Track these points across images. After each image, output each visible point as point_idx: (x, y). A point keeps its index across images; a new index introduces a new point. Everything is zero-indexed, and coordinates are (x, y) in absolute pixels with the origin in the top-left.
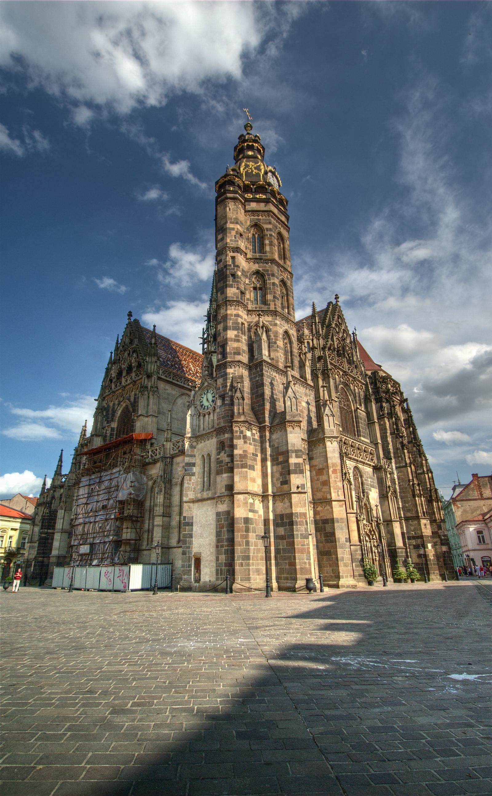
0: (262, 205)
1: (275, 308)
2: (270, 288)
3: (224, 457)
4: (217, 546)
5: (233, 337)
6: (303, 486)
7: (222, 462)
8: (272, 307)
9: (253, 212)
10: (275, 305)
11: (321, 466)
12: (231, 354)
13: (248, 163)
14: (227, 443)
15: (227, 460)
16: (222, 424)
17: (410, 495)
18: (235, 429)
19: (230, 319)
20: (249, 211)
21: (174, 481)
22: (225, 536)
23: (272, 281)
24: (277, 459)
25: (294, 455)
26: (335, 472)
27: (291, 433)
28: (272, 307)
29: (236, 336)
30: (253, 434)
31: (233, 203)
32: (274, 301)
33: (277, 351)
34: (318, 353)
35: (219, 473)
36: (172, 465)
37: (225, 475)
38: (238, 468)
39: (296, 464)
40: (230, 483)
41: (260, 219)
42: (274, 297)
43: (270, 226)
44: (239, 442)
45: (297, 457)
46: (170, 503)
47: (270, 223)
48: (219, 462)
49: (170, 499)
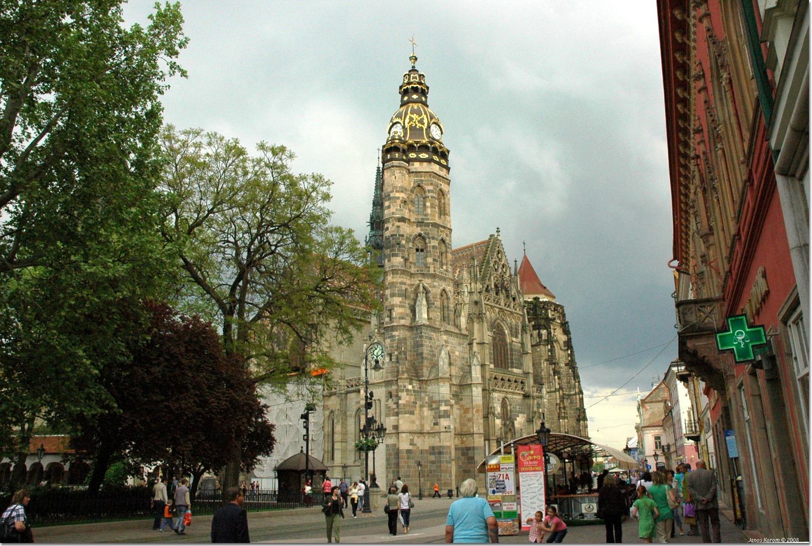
0: (425, 164)
1: (434, 271)
2: (430, 252)
3: (391, 403)
4: (387, 468)
5: (398, 303)
6: (449, 427)
7: (389, 407)
8: (432, 271)
9: (417, 173)
10: (434, 267)
11: (468, 406)
12: (396, 318)
13: (412, 116)
14: (394, 393)
15: (395, 406)
16: (390, 378)
17: (556, 417)
18: (400, 384)
19: (396, 287)
20: (413, 172)
21: (348, 413)
22: (393, 461)
23: (432, 244)
24: (431, 406)
25: (443, 404)
26: (477, 411)
27: (442, 386)
28: (432, 271)
29: (400, 302)
30: (413, 387)
31: (398, 171)
32: (433, 264)
33: (436, 312)
34: (476, 297)
35: (387, 415)
36: (346, 399)
37: (392, 418)
38: (402, 414)
39: (444, 411)
40: (396, 424)
41: (421, 181)
42: (434, 260)
43: (431, 188)
44: (403, 395)
45: (446, 405)
46: (346, 431)
47: (432, 184)
48: (388, 407)
49: (346, 428)
